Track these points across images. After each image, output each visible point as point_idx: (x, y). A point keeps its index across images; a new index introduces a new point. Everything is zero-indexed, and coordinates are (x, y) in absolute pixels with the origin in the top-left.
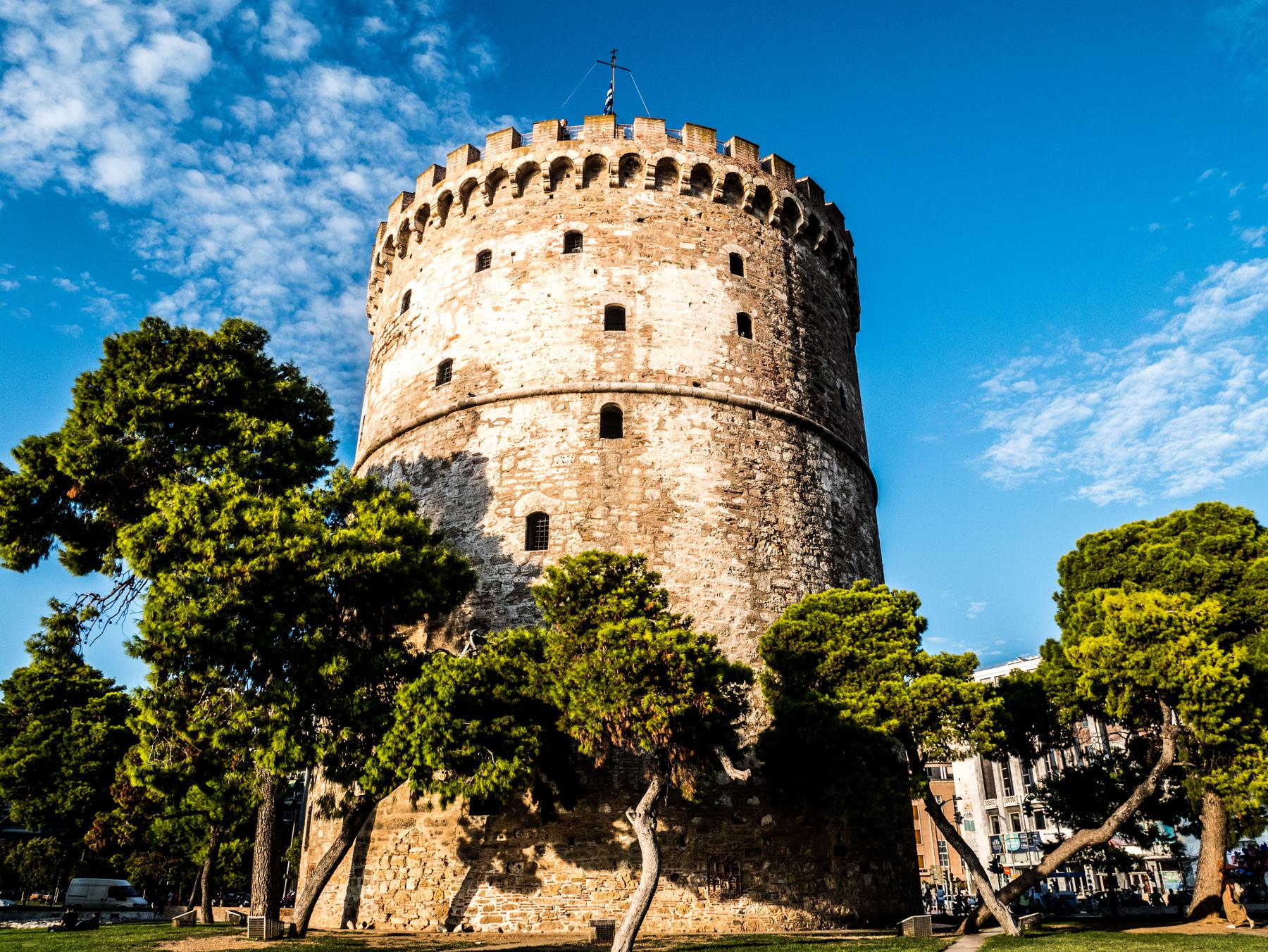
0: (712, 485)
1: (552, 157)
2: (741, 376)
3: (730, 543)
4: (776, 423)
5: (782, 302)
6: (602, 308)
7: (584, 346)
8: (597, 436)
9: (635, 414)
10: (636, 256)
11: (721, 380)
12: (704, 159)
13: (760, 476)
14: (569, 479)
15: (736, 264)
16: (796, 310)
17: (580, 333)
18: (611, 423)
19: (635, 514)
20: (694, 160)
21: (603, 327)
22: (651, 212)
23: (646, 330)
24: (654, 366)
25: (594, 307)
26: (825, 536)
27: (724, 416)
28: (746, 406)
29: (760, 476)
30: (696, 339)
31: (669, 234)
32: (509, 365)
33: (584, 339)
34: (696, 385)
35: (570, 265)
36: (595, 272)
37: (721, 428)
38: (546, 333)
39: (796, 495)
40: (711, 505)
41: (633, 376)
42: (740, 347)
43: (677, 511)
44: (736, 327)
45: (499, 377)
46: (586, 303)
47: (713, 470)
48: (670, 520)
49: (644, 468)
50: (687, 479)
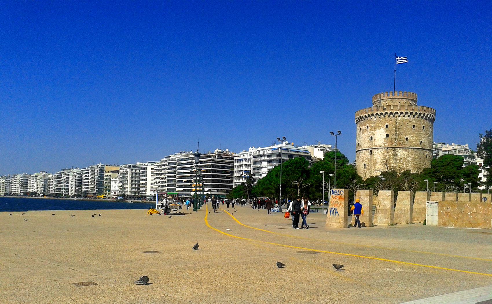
0: (381, 159)
1: (364, 115)
2: (386, 144)
4: (391, 149)
6: (370, 137)
12: (381, 112)
13: (388, 157)
15: (387, 126)
20: (380, 113)
21: (370, 140)
22: (376, 121)
23: (375, 140)
24: (375, 145)
26: (398, 162)
27: (383, 150)
28: (386, 148)
29: (388, 157)
34: (380, 146)
39: (393, 158)
41: (373, 146)
46: (369, 137)
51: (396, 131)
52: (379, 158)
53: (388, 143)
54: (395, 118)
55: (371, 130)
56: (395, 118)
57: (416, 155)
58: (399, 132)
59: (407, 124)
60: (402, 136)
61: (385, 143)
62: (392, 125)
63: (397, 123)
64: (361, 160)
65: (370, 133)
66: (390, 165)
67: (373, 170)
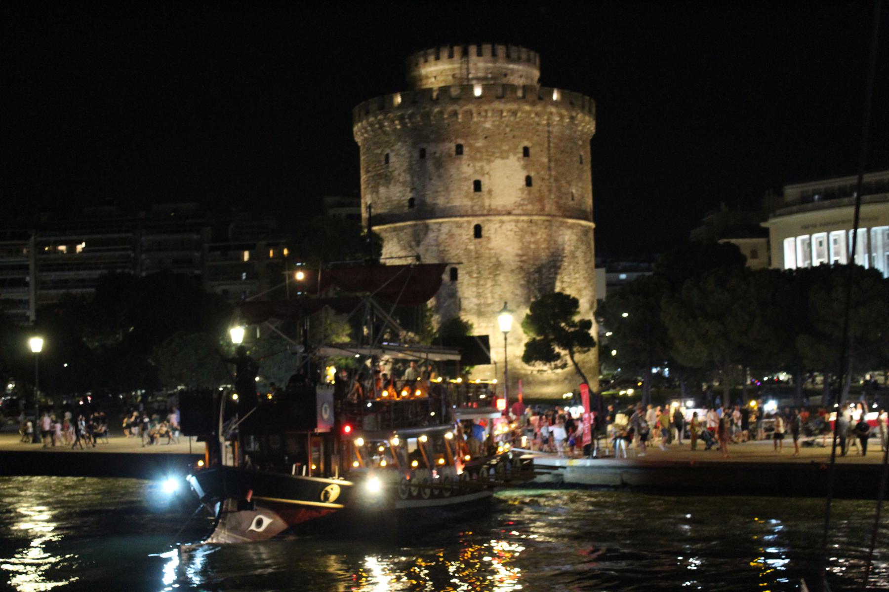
2: (526, 205)
6: (472, 181)
10: (485, 157)
11: (518, 209)
13: (533, 246)
15: (526, 152)
16: (552, 165)
18: (478, 231)
23: (490, 192)
24: (493, 207)
27: (520, 225)
29: (533, 246)
33: (466, 196)
36: (469, 165)
49: (490, 249)
53: (532, 203)
54: (546, 128)
55: (473, 159)
56: (546, 128)
63: (552, 145)
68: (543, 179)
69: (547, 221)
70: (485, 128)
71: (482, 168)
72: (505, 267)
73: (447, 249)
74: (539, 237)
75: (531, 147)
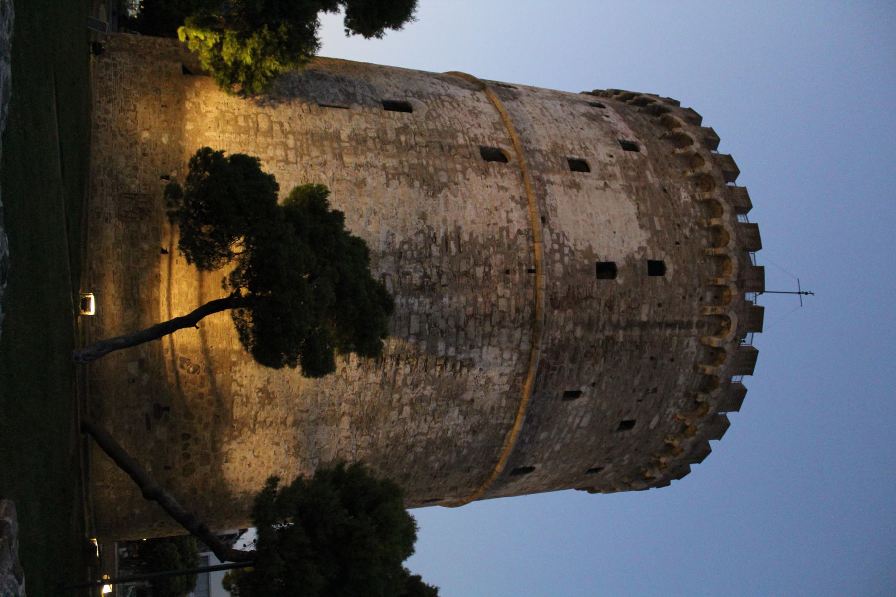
2: (561, 260)
3: (417, 234)
5: (640, 313)
6: (584, 157)
7: (549, 144)
8: (481, 144)
9: (505, 170)
10: (634, 184)
11: (553, 242)
13: (480, 271)
14: (442, 125)
15: (656, 268)
17: (560, 142)
19: (424, 162)
21: (569, 156)
23: (576, 186)
24: (548, 188)
25: (583, 152)
26: (441, 346)
27: (522, 241)
29: (480, 271)
30: (581, 223)
31: (661, 210)
32: (519, 104)
33: (555, 144)
35: (610, 143)
36: (611, 156)
37: (512, 237)
38: (552, 125)
39: (470, 310)
40: (444, 221)
42: (586, 262)
43: (434, 195)
44: (603, 260)
45: (510, 101)
47: (475, 226)
48: (425, 187)
50: (461, 202)
51: (630, 325)
52: (470, 213)
53: (567, 274)
55: (624, 164)
56: (695, 319)
57: (465, 451)
58: (623, 344)
59: (655, 390)
60: (599, 368)
61: (563, 255)
62: (663, 297)
63: (668, 332)
64: (430, 90)
65: (608, 159)
66: (421, 288)
67: (379, 163)
68: (610, 306)
69: (533, 315)
70: (679, 189)
71: (612, 176)
72: (430, 201)
73: (446, 104)
74: (500, 290)
75: (665, 279)
